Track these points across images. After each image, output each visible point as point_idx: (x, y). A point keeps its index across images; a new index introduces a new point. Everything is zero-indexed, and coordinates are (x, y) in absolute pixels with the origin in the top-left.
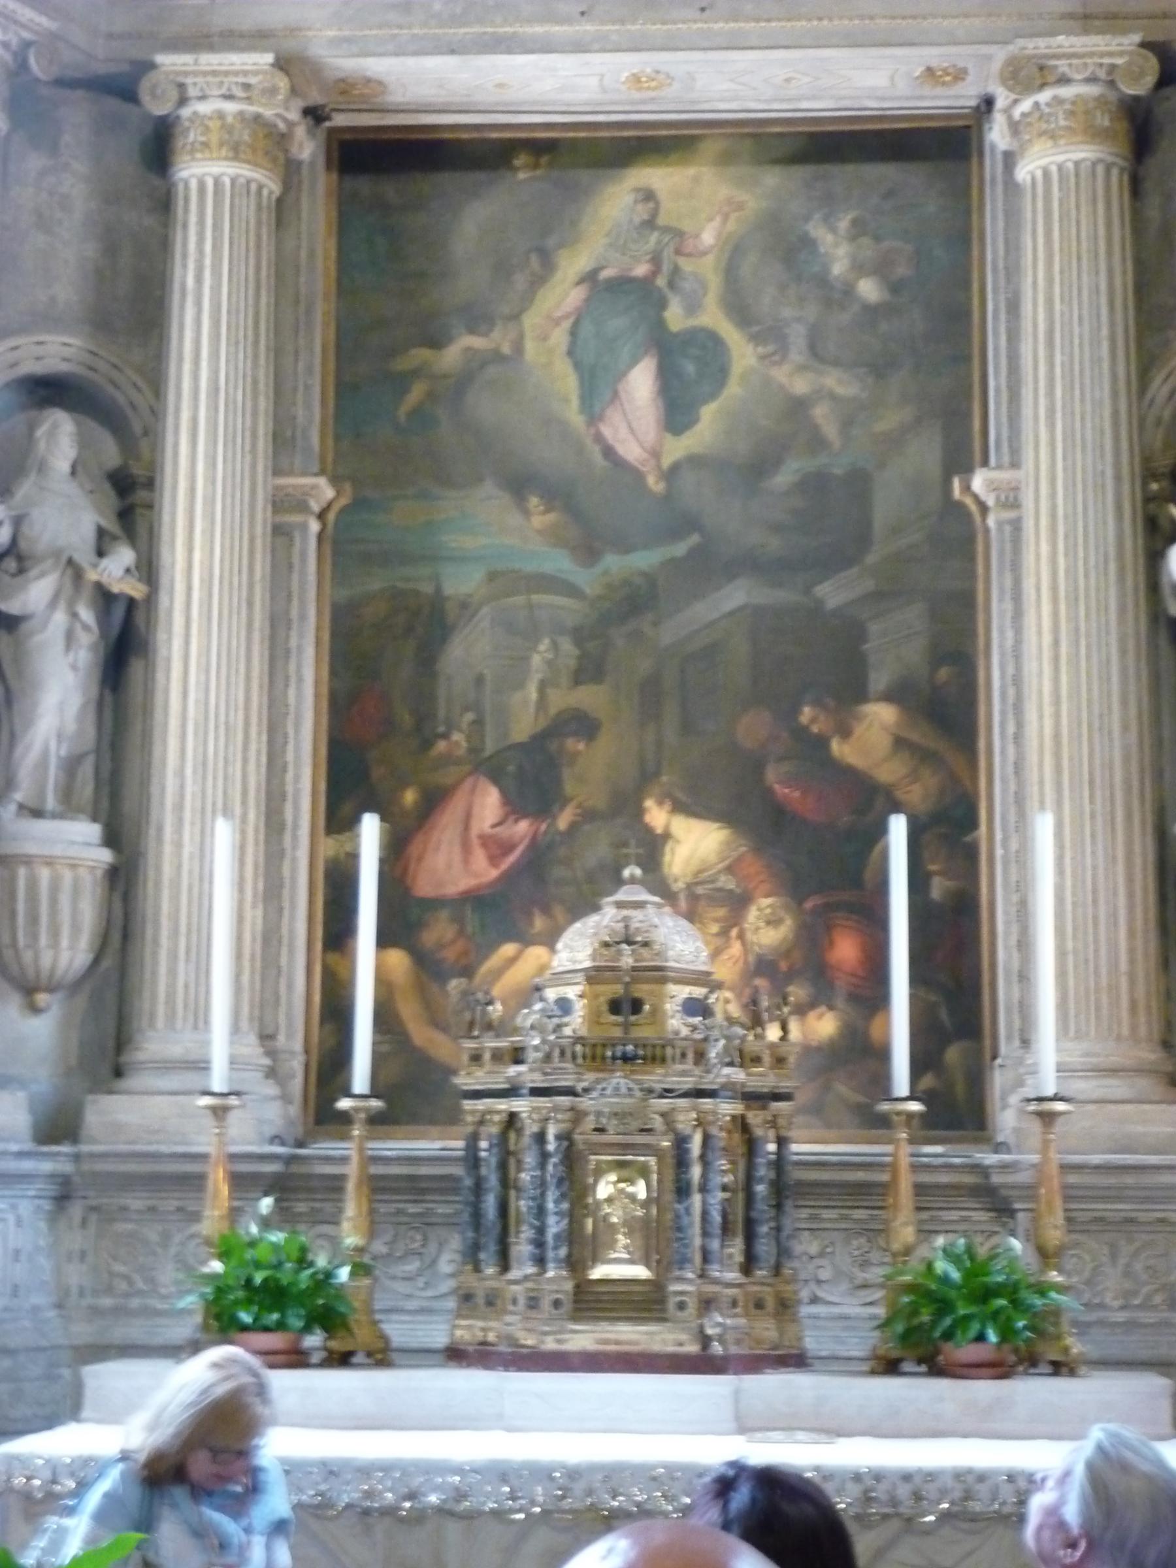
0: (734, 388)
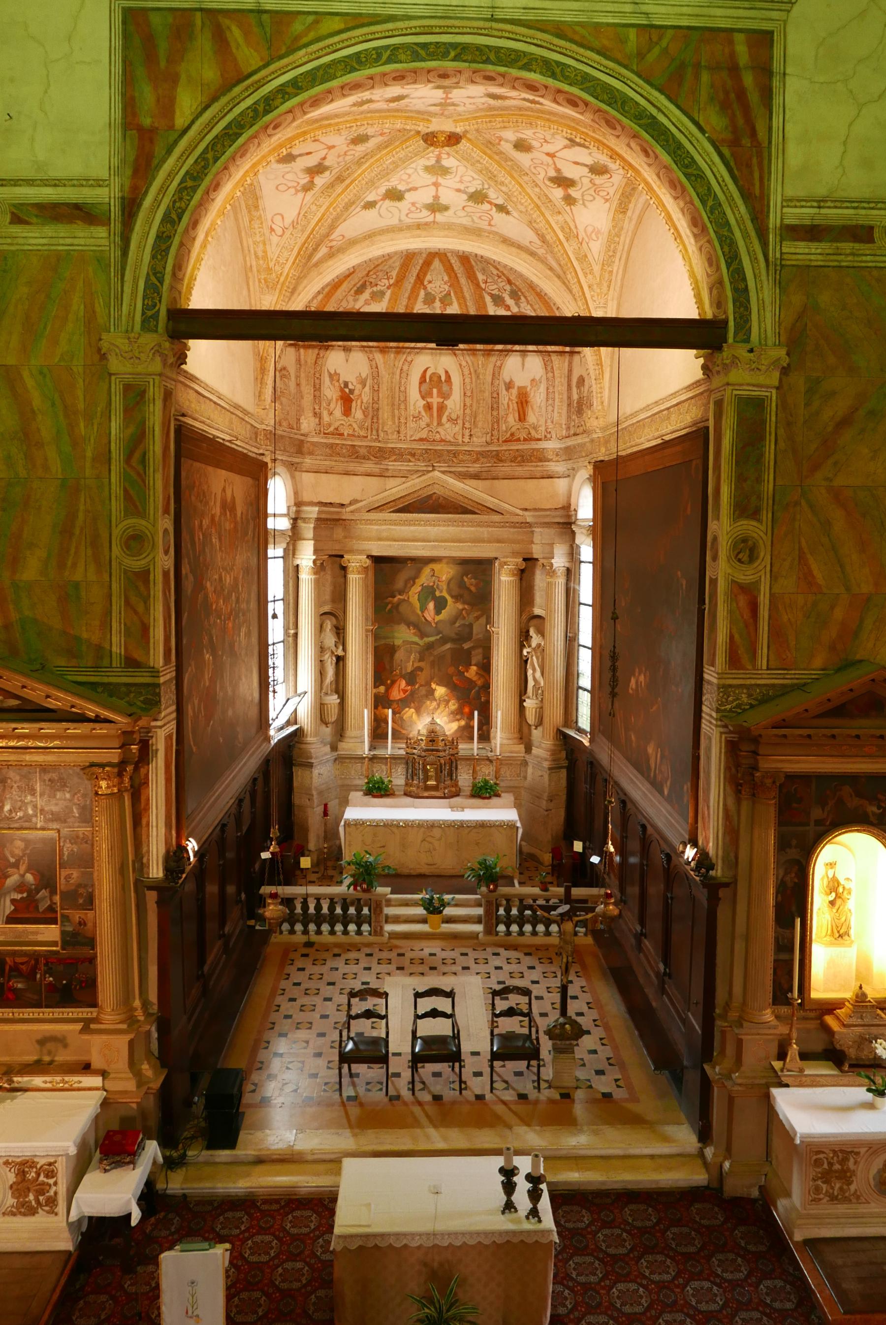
0: (448, 608)
